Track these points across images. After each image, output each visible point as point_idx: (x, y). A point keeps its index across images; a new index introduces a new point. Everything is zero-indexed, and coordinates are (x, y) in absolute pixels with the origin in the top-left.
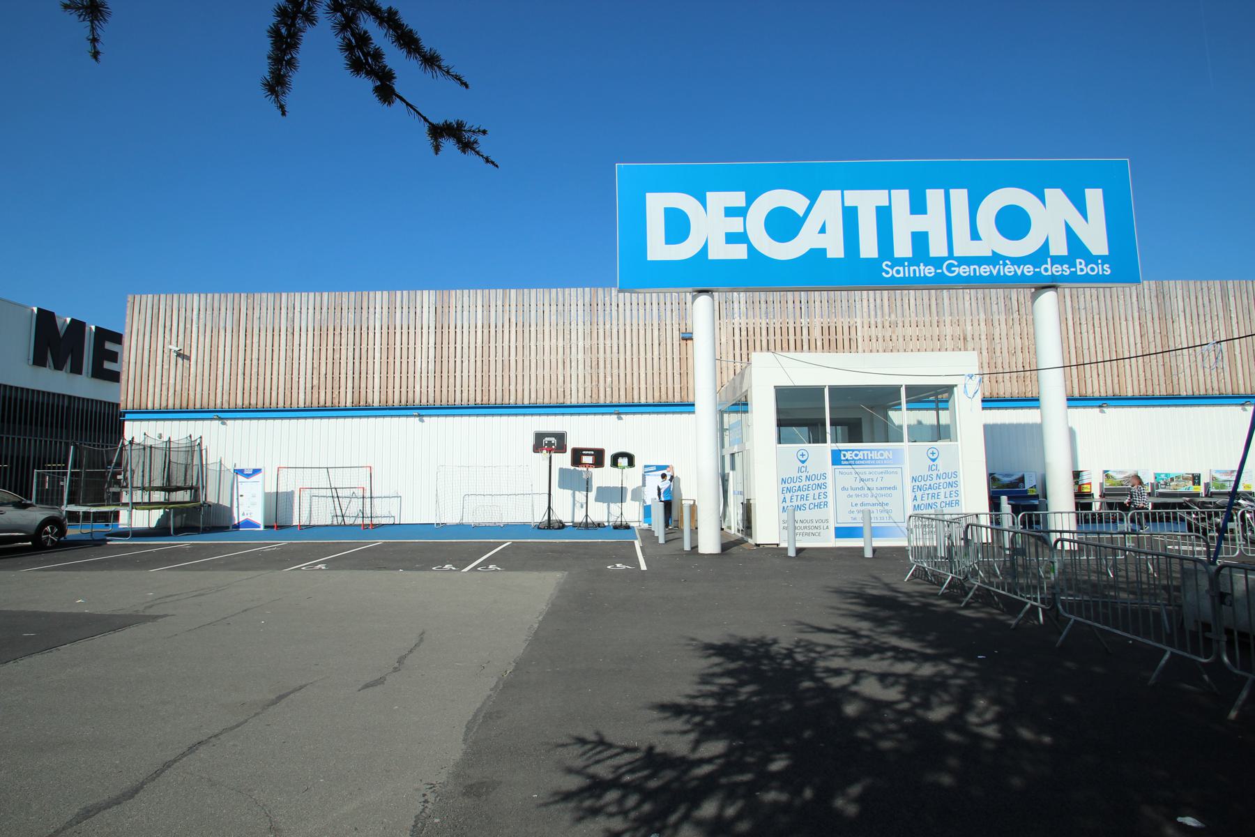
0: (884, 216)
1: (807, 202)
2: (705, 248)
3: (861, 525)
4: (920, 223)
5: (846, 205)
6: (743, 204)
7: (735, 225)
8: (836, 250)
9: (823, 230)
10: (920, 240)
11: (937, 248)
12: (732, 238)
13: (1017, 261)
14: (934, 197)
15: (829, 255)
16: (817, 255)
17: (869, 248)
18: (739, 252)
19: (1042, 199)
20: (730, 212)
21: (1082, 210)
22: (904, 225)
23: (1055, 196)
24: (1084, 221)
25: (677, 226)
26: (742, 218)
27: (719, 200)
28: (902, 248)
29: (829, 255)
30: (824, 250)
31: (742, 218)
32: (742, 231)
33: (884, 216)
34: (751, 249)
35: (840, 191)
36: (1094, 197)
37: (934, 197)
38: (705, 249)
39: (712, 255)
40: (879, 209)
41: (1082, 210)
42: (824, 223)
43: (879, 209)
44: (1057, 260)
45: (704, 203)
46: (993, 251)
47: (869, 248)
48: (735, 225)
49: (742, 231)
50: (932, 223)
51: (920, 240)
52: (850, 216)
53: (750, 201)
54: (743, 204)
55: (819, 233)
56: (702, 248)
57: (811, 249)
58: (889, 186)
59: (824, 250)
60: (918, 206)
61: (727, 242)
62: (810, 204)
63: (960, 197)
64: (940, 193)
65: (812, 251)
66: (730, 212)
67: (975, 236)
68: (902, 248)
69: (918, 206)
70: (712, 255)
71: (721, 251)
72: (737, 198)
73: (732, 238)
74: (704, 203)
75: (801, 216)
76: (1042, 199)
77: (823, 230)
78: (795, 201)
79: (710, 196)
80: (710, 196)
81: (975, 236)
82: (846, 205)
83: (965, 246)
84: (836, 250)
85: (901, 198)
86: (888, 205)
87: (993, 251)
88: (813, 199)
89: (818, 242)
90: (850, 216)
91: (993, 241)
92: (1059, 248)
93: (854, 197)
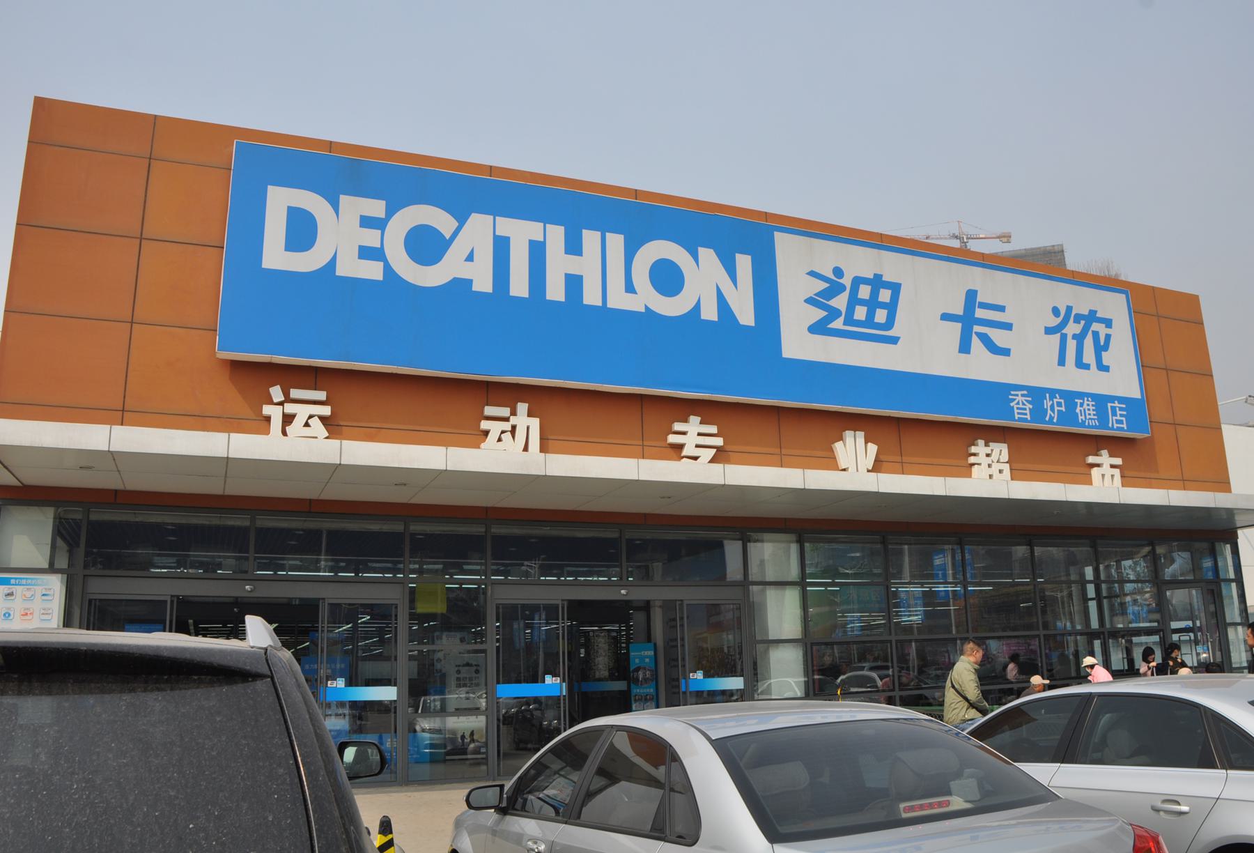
0: (537, 251)
1: (457, 224)
2: (333, 261)
4: (573, 265)
5: (498, 233)
6: (383, 215)
7: (371, 238)
8: (483, 283)
9: (470, 258)
10: (574, 283)
11: (591, 297)
12: (366, 253)
14: (590, 238)
16: (459, 286)
17: (519, 287)
18: (372, 271)
20: (367, 222)
22: (558, 265)
27: (355, 206)
28: (555, 291)
30: (470, 281)
31: (380, 231)
32: (378, 246)
33: (537, 251)
34: (388, 269)
35: (492, 217)
37: (590, 238)
38: (333, 261)
39: (341, 271)
40: (532, 243)
42: (472, 250)
43: (532, 243)
45: (336, 207)
47: (519, 287)
48: (371, 238)
49: (378, 246)
50: (587, 266)
51: (574, 283)
52: (501, 246)
53: (390, 212)
54: (383, 215)
55: (465, 261)
56: (331, 260)
57: (454, 278)
58: (546, 219)
59: (470, 281)
60: (573, 247)
61: (360, 257)
62: (458, 227)
63: (616, 242)
65: (456, 281)
66: (367, 222)
67: (630, 288)
68: (555, 291)
69: (573, 247)
70: (341, 271)
71: (352, 267)
72: (376, 208)
73: (366, 253)
74: (336, 207)
75: (447, 238)
77: (470, 258)
78: (442, 221)
79: (344, 200)
80: (344, 200)
81: (630, 288)
82: (497, 233)
83: (619, 300)
84: (483, 283)
85: (556, 235)
86: (542, 240)
87: (646, 306)
88: (462, 220)
89: (465, 271)
90: (501, 246)
91: (647, 298)
92: (710, 313)
93: (507, 226)
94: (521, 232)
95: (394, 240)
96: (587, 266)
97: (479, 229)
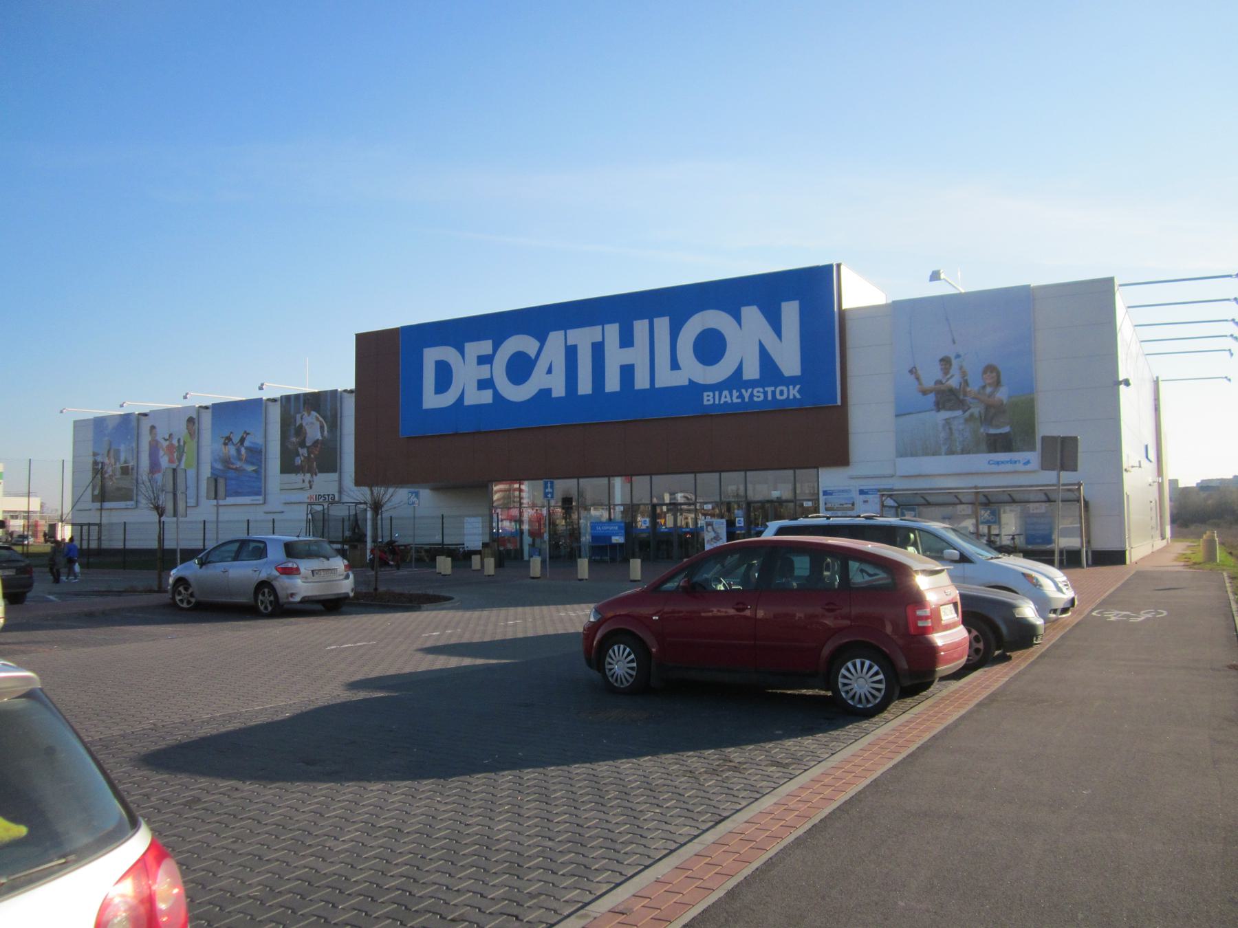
0: (598, 350)
1: (537, 344)
3: (1128, 561)
5: (569, 344)
6: (490, 352)
7: (484, 372)
8: (559, 391)
9: (549, 371)
10: (627, 372)
13: (717, 387)
14: (640, 327)
15: (554, 395)
16: (545, 393)
17: (585, 386)
18: (486, 397)
19: (738, 318)
21: (777, 329)
22: (615, 358)
23: (751, 314)
24: (779, 341)
25: (444, 375)
26: (489, 365)
27: (475, 348)
28: (613, 383)
29: (554, 395)
30: (549, 391)
33: (598, 350)
34: (497, 395)
36: (790, 312)
39: (467, 402)
41: (777, 329)
44: (752, 384)
45: (462, 351)
46: (690, 381)
47: (585, 386)
49: (489, 377)
50: (637, 355)
51: (627, 372)
52: (571, 353)
53: (496, 348)
54: (490, 352)
59: (549, 391)
60: (627, 340)
63: (663, 325)
64: (646, 322)
67: (675, 365)
68: (613, 383)
69: (627, 340)
70: (468, 401)
72: (485, 347)
74: (462, 351)
76: (738, 318)
77: (549, 371)
81: (675, 365)
83: (667, 379)
84: (559, 391)
87: (690, 380)
88: (542, 340)
91: (692, 371)
92: (752, 371)
94: (583, 337)
95: (499, 371)
96: (637, 355)
97: (556, 340)
